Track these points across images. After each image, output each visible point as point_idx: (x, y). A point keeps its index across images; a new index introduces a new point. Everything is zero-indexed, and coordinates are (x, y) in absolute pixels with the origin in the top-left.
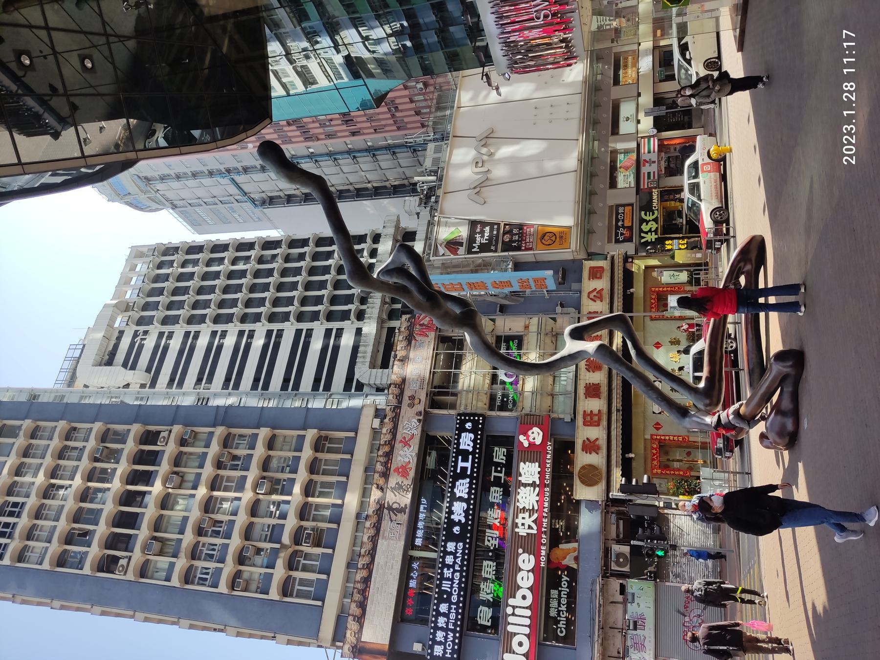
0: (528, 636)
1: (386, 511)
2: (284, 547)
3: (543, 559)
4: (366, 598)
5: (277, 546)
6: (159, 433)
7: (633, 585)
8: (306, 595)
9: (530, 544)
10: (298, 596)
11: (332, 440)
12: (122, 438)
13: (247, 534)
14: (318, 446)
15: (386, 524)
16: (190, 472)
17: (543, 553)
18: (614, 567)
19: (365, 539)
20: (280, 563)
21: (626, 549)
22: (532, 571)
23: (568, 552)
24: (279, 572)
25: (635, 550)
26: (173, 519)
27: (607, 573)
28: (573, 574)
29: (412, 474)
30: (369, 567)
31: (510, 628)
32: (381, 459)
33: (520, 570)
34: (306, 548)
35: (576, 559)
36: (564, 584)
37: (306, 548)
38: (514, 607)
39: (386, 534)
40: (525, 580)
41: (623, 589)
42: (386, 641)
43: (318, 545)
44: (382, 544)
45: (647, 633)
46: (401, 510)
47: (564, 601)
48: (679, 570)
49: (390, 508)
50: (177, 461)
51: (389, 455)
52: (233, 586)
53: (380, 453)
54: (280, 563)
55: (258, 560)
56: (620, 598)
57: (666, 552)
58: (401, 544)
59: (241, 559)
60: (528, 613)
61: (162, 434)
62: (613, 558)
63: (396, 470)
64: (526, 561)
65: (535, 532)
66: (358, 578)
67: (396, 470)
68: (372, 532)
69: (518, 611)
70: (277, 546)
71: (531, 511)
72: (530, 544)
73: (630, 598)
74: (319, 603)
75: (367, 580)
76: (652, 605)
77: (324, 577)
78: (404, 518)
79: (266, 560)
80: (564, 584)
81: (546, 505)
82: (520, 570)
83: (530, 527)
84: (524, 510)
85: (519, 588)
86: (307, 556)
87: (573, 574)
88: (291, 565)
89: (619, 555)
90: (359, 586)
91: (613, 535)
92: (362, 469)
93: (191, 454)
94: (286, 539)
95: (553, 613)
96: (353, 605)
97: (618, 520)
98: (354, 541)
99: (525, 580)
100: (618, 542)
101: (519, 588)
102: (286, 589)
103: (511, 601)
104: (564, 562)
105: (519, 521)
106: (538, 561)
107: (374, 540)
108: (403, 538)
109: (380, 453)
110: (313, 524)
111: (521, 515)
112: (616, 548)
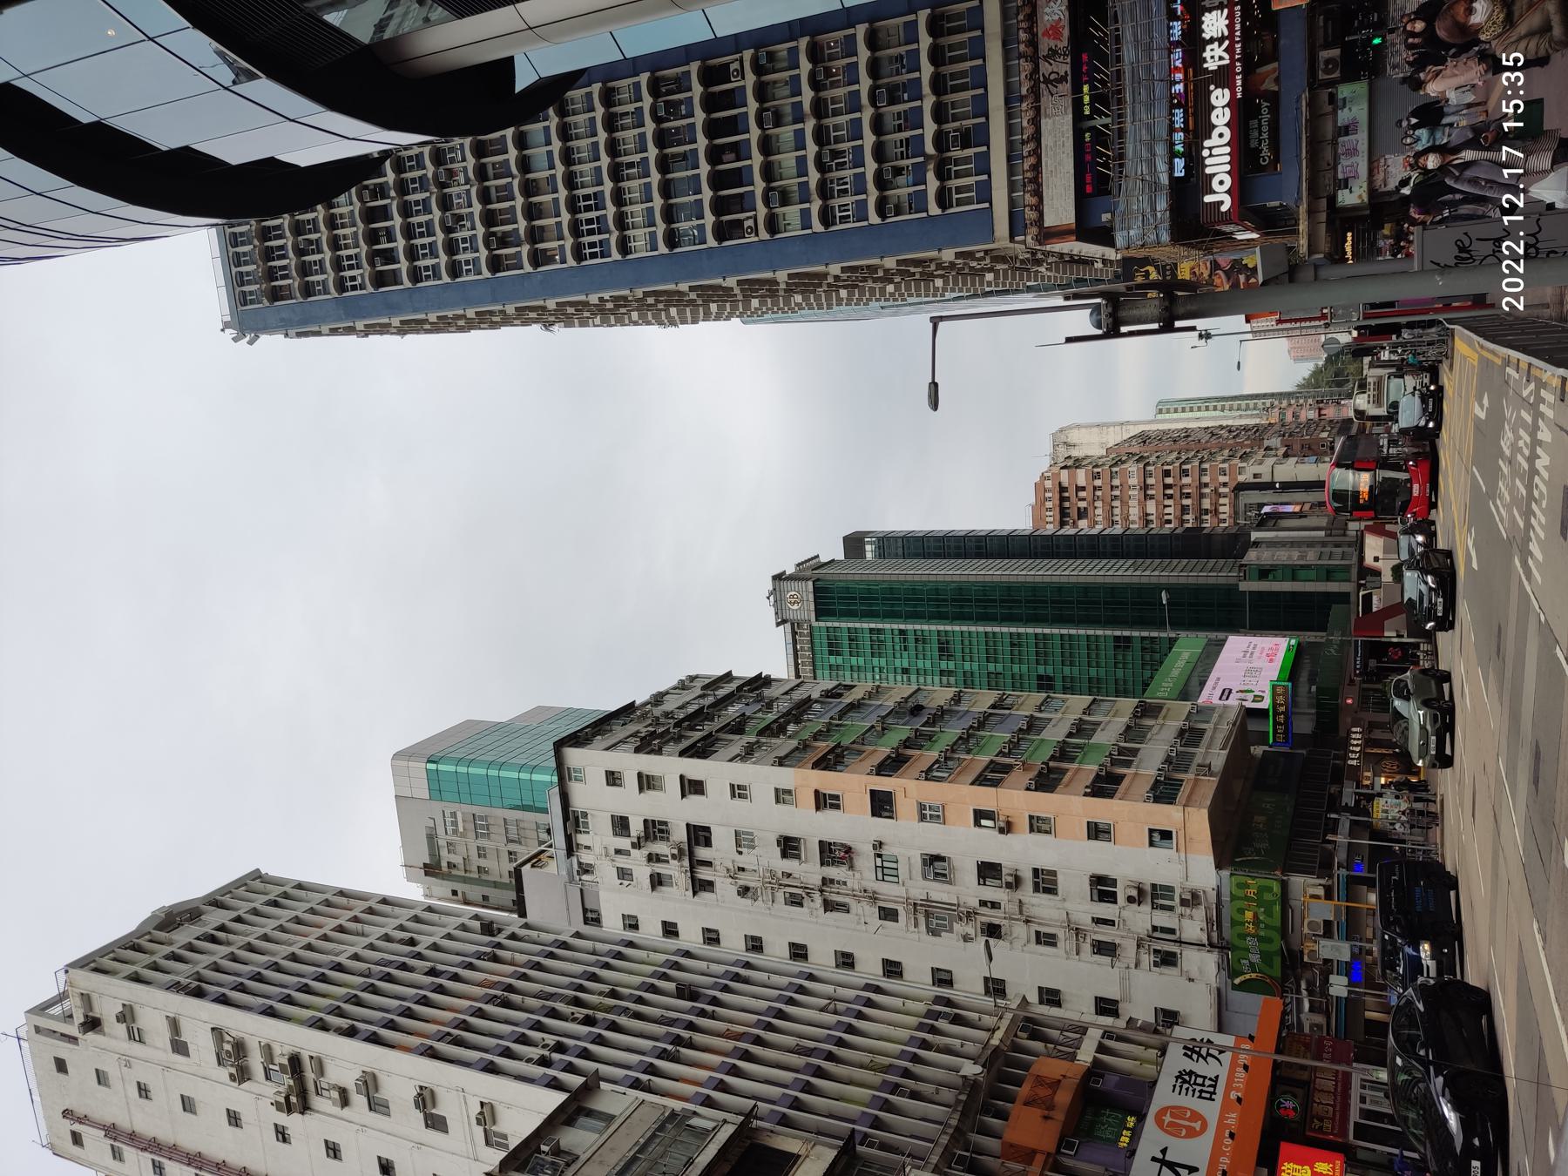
0: (1228, 173)
1: (1043, 86)
2: (928, 157)
3: (1239, 89)
4: (1040, 185)
5: (921, 159)
6: (727, 65)
7: (1344, 91)
8: (969, 201)
9: (1223, 77)
10: (960, 203)
11: (950, 18)
12: (682, 84)
13: (879, 153)
14: (935, 28)
15: (1046, 100)
16: (785, 104)
17: (1239, 83)
18: (1322, 76)
19: (1025, 124)
20: (930, 176)
21: (1335, 53)
22: (1228, 105)
23: (1268, 74)
24: (933, 184)
25: (1347, 49)
26: (784, 164)
27: (1314, 85)
28: (1274, 98)
29: (1066, 33)
30: (1037, 153)
31: (1208, 171)
32: (1023, 25)
33: (1214, 108)
34: (957, 153)
35: (1277, 80)
36: (1265, 111)
37: (957, 153)
38: (1210, 149)
39: (1049, 111)
40: (1221, 118)
41: (1332, 98)
42: (1073, 220)
43: (966, 145)
44: (1046, 124)
45: (1361, 139)
46: (1062, 79)
47: (1265, 129)
48: (1398, 59)
49: (1047, 81)
50: (762, 93)
51: (1032, 18)
52: (881, 212)
53: (1021, 17)
54: (930, 176)
55: (901, 180)
56: (1330, 108)
57: (1384, 38)
58: (1069, 117)
59: (881, 183)
60: (1228, 150)
61: (733, 66)
62: (1322, 66)
63: (1046, 33)
64: (1220, 97)
65: (1227, 62)
66: (1026, 167)
67: (1046, 33)
68: (1031, 114)
69: (1215, 152)
70: (921, 159)
71: (1221, 40)
72: (1223, 77)
73: (1340, 104)
74: (987, 205)
75: (1037, 167)
76: (1365, 106)
77: (985, 177)
78: (1066, 87)
79: (910, 178)
80: (1265, 111)
81: (1238, 27)
82: (1214, 108)
83: (1221, 58)
84: (1212, 40)
85: (1214, 127)
86: (957, 162)
87: (1274, 98)
88: (942, 175)
89: (1327, 62)
90: (1029, 175)
91: (1321, 41)
92: (999, 43)
93: (775, 82)
94: (930, 149)
95: (1254, 144)
96: (1027, 196)
97: (1326, 21)
98: (1010, 130)
99: (1221, 118)
100: (1327, 46)
101: (1214, 127)
102: (943, 199)
103: (1207, 143)
104: (1263, 87)
105: (1207, 54)
106: (1233, 94)
107: (1036, 122)
108: (1070, 110)
109: (1021, 17)
110: (957, 124)
111: (1208, 48)
112: (1325, 54)
